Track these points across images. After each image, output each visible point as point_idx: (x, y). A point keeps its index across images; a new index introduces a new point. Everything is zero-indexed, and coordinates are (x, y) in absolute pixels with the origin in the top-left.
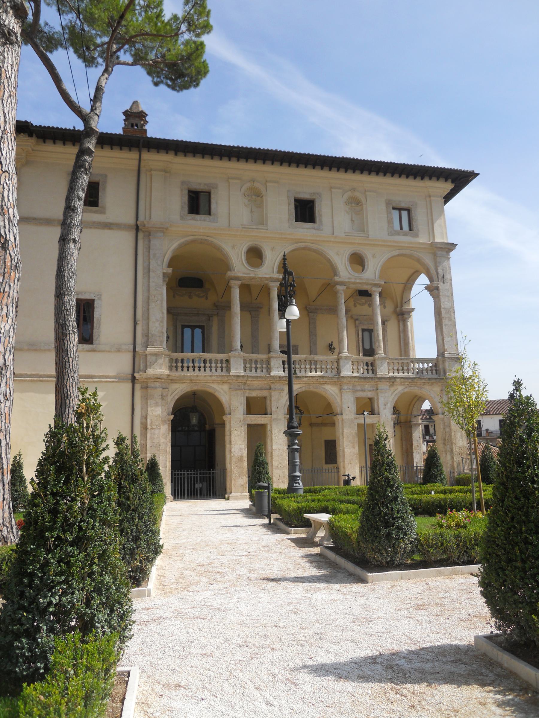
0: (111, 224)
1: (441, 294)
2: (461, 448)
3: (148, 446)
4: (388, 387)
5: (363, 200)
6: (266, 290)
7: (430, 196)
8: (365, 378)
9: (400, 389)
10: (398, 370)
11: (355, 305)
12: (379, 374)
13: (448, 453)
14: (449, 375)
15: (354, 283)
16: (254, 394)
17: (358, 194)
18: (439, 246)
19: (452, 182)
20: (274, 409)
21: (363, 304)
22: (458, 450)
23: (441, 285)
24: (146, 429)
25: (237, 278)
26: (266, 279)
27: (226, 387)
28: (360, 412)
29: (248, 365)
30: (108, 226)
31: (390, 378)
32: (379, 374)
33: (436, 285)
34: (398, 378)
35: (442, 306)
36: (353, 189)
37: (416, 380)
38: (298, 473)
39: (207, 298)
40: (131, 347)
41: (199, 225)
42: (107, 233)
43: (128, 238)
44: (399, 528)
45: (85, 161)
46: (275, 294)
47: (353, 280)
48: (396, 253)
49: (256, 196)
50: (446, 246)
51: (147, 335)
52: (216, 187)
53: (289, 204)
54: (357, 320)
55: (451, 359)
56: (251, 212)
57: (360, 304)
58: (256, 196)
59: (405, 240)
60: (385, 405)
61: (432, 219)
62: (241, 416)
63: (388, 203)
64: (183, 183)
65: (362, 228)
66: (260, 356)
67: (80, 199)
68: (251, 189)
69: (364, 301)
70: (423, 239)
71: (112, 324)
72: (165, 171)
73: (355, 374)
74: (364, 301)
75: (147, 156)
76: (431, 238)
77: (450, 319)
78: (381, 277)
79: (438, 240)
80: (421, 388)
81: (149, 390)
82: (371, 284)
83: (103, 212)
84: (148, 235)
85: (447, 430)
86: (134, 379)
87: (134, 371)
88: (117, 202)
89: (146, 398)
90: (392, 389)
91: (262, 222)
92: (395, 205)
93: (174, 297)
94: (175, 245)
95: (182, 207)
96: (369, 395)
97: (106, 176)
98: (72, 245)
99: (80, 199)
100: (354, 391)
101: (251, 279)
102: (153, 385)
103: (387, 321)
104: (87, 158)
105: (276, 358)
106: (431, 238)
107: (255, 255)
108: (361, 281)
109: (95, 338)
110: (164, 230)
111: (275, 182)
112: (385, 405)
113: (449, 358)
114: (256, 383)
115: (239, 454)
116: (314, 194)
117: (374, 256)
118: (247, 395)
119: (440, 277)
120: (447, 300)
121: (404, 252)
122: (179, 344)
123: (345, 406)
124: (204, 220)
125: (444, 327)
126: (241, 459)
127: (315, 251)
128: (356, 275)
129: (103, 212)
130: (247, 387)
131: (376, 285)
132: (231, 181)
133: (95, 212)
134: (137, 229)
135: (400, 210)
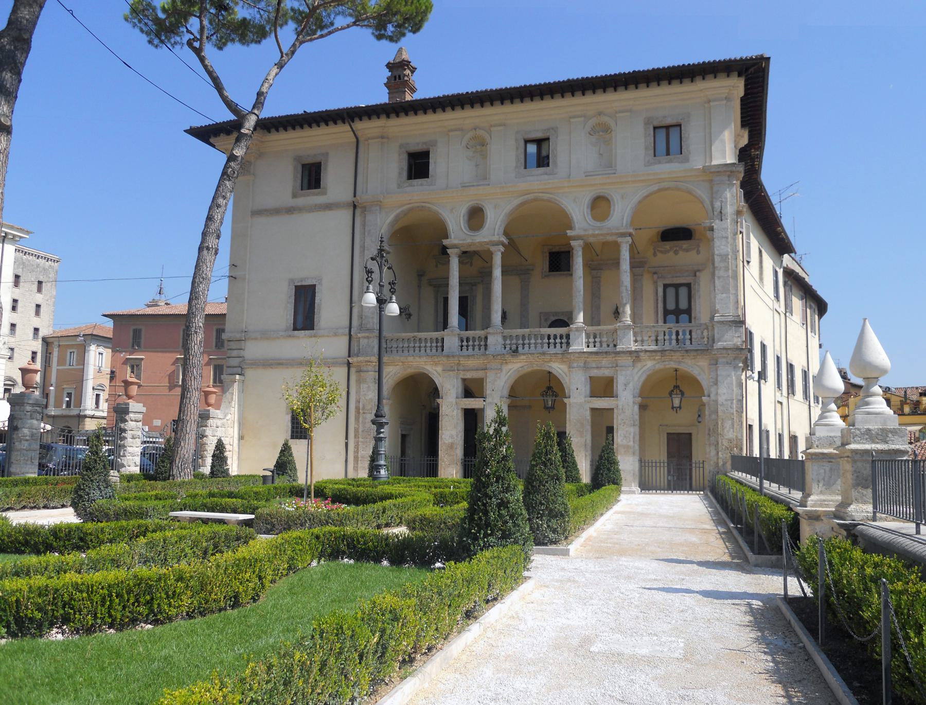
0: (331, 204)
1: (716, 234)
2: (730, 441)
3: (360, 431)
4: (631, 364)
5: (612, 125)
6: (490, 254)
7: (709, 101)
8: (596, 353)
9: (649, 365)
10: (642, 341)
11: (655, 255)
12: (619, 348)
13: (713, 448)
14: (719, 344)
15: (593, 235)
16: (469, 375)
17: (606, 119)
18: (713, 170)
19: (740, 75)
20: (488, 391)
21: (668, 251)
22: (726, 443)
23: (717, 224)
24: (359, 413)
25: (455, 246)
26: (487, 243)
27: (439, 369)
28: (593, 394)
29: (465, 343)
30: (328, 207)
31: (631, 352)
32: (620, 347)
33: (708, 225)
34: (642, 351)
35: (716, 252)
36: (600, 114)
37: (667, 353)
38: (382, 462)
39: (471, 265)
40: (347, 331)
41: (418, 192)
42: (329, 214)
43: (343, 217)
44: (81, 496)
45: (230, 167)
46: (497, 260)
47: (590, 232)
48: (655, 188)
49: (479, 145)
50: (725, 169)
51: (361, 317)
52: (434, 143)
53: (517, 149)
54: (655, 273)
55: (722, 322)
56: (477, 165)
57: (661, 252)
58: (479, 145)
59: (668, 169)
60: (625, 385)
61: (710, 133)
62: (454, 400)
63: (647, 122)
64: (401, 146)
65: (609, 165)
66: (477, 332)
67: (219, 206)
68: (474, 138)
69: (668, 247)
70: (697, 163)
71: (331, 309)
72: (382, 137)
73: (592, 349)
74: (668, 247)
75: (359, 125)
76: (708, 160)
77: (727, 269)
78: (632, 223)
79: (715, 162)
80: (679, 362)
81: (362, 374)
82: (617, 234)
83: (325, 193)
84: (364, 209)
85: (714, 416)
86: (349, 364)
87: (349, 356)
88: (337, 182)
89: (359, 382)
90: (639, 365)
91: (483, 178)
92: (656, 124)
93: (436, 266)
94: (391, 217)
95: (400, 173)
96: (607, 373)
97: (327, 154)
98: (205, 252)
99: (219, 206)
100: (586, 367)
101: (469, 245)
102: (365, 369)
103: (699, 271)
104: (232, 164)
105: (493, 334)
106: (708, 160)
107: (476, 216)
108: (600, 232)
109: (315, 323)
110: (379, 204)
111: (500, 125)
112: (625, 385)
113: (719, 322)
114: (471, 363)
115: (450, 441)
116: (548, 129)
117: (622, 197)
118: (463, 375)
119: (716, 213)
120: (724, 243)
121: (665, 185)
122: (441, 319)
123: (573, 388)
124: (422, 185)
125: (717, 282)
126: (451, 446)
127: (549, 201)
128: (598, 224)
129: (325, 193)
130: (462, 368)
131: (623, 235)
132: (451, 134)
133: (317, 194)
134: (355, 207)
135: (667, 127)
